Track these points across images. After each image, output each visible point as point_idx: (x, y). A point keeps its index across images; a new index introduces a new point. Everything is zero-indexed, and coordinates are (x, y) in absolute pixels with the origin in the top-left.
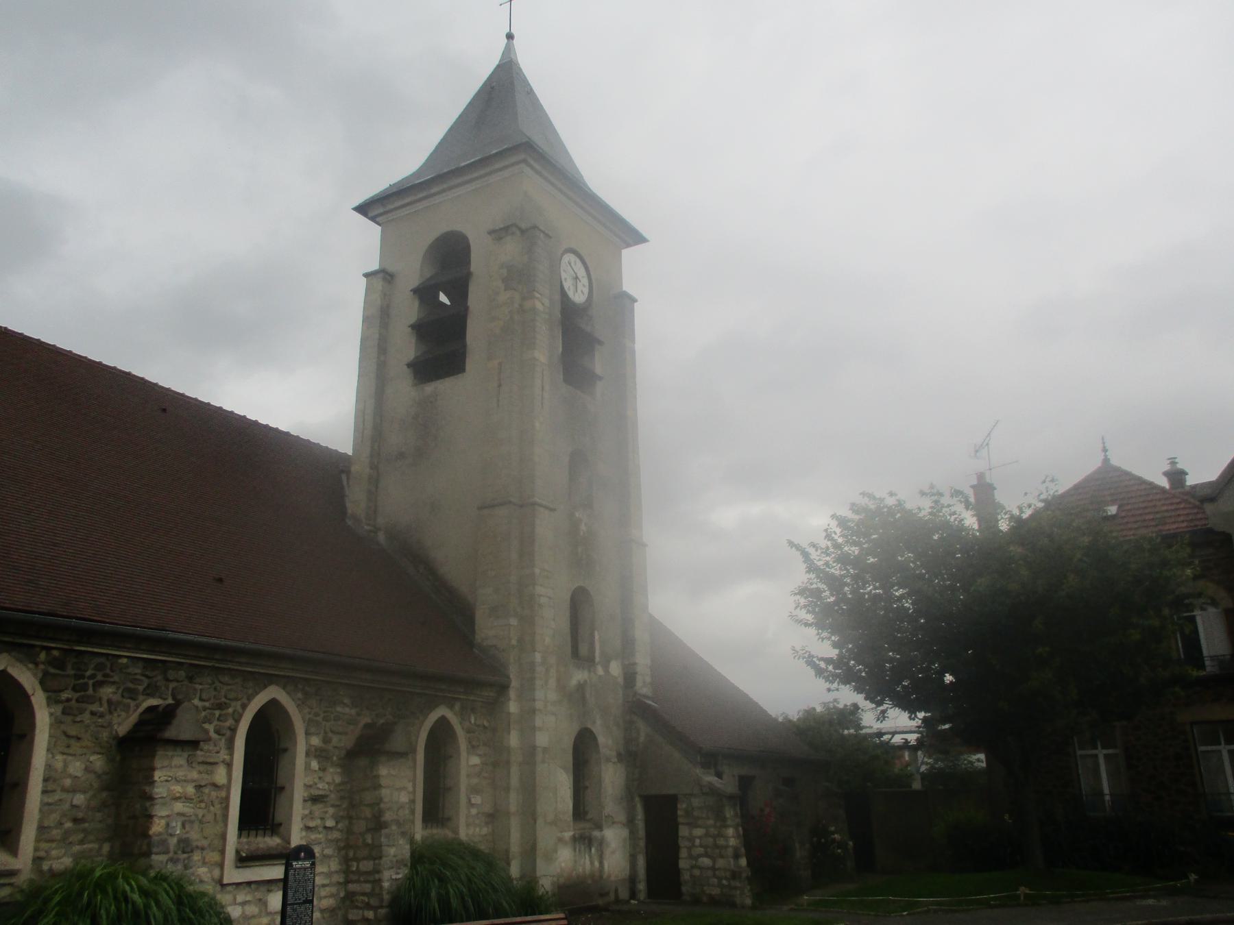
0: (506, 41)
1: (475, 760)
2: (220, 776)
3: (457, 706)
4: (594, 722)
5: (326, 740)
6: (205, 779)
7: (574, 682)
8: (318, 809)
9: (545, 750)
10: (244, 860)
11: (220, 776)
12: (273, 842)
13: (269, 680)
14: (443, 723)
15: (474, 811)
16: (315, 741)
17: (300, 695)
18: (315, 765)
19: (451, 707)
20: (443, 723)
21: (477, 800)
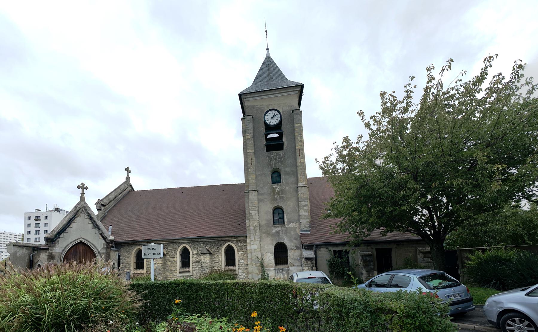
0: (268, 47)
1: (240, 253)
2: (175, 259)
3: (234, 242)
4: (284, 240)
5: (198, 252)
6: (172, 260)
7: (274, 231)
8: (197, 264)
9: (255, 249)
10: (180, 272)
11: (175, 259)
12: (187, 269)
13: (182, 243)
14: (229, 246)
15: (241, 264)
16: (195, 252)
17: (190, 245)
18: (195, 256)
19: (232, 242)
20: (229, 246)
21: (243, 261)
